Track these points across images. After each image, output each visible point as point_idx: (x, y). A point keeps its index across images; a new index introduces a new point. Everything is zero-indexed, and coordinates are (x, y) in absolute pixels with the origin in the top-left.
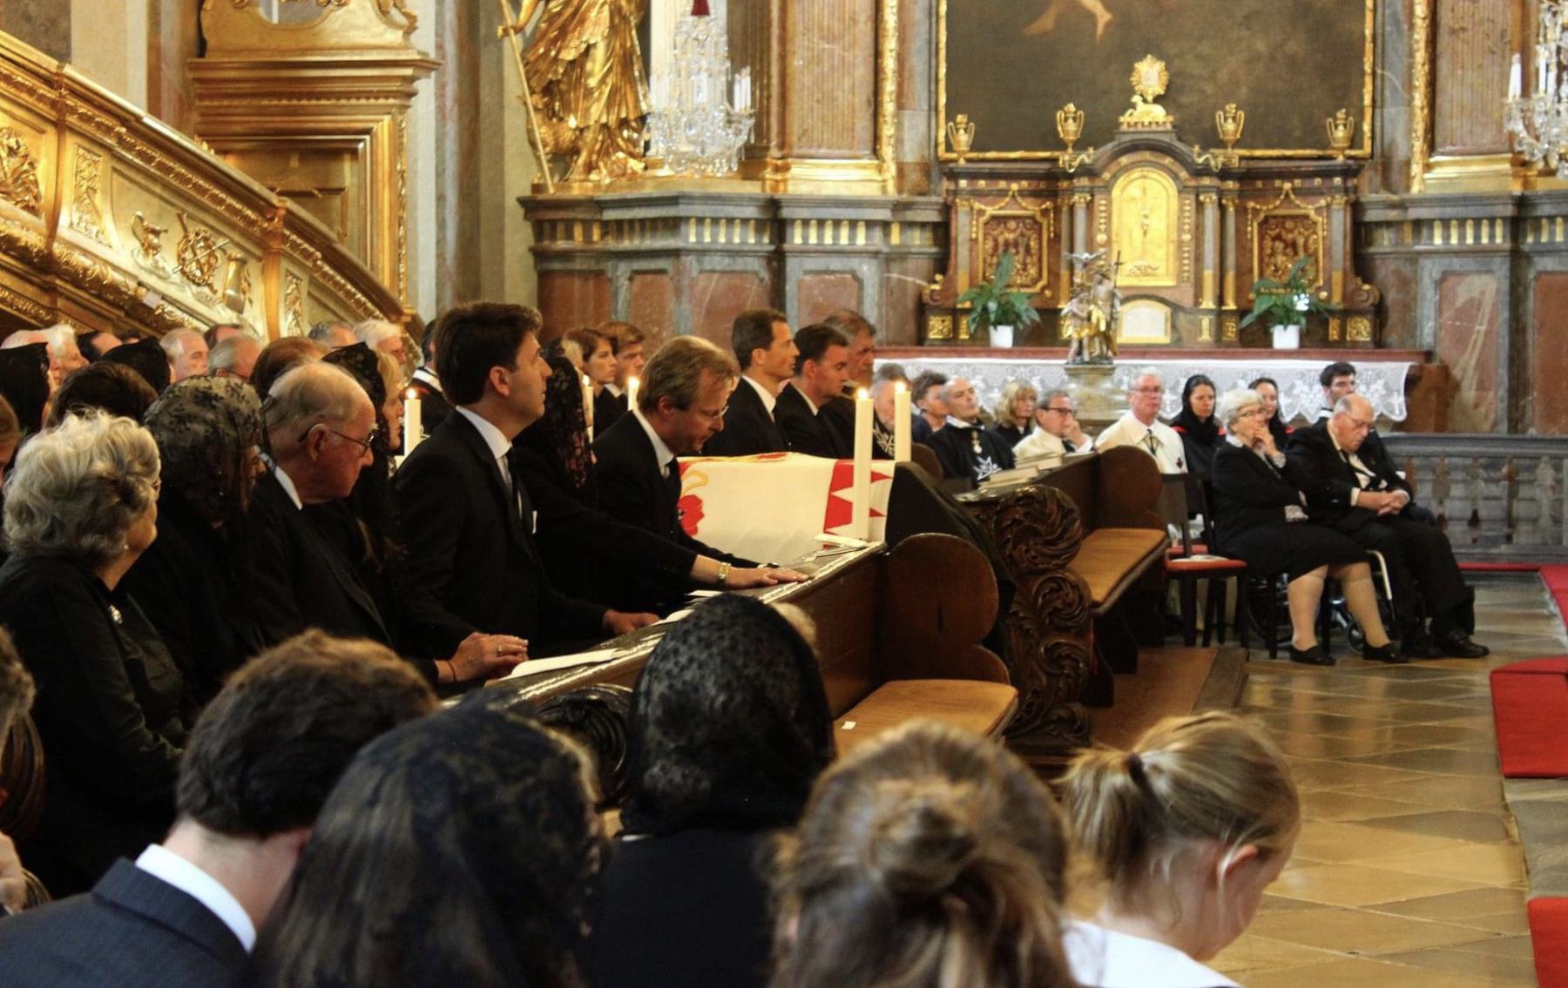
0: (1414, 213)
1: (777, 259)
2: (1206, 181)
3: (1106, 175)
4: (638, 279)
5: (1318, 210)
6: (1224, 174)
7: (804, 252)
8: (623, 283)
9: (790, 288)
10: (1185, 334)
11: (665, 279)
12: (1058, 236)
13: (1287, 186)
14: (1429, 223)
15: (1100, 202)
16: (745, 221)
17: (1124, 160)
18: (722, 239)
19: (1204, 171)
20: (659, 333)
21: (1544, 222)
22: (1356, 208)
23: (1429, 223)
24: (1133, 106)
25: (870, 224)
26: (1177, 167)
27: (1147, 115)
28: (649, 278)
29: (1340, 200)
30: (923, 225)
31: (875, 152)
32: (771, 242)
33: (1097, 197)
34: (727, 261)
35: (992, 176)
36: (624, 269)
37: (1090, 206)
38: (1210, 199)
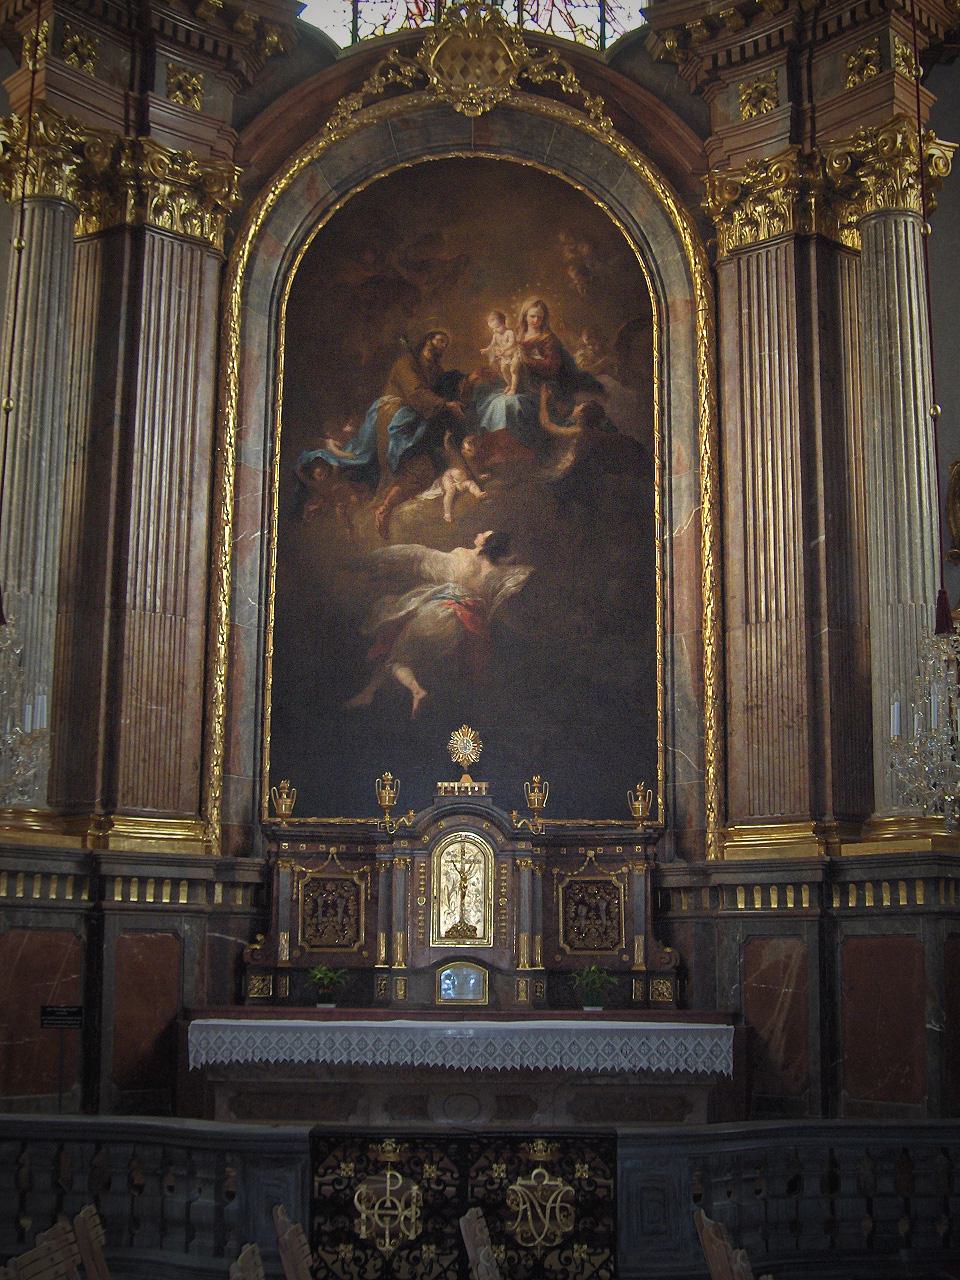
0: (716, 879)
2: (522, 845)
5: (620, 877)
6: (536, 841)
7: (124, 909)
12: (375, 898)
13: (591, 853)
14: (732, 889)
16: (62, 877)
17: (443, 823)
19: (515, 836)
21: (852, 887)
22: (655, 875)
23: (732, 889)
25: (192, 883)
26: (494, 830)
29: (640, 869)
30: (246, 885)
31: (201, 813)
32: (91, 899)
33: (417, 859)
35: (313, 839)
37: (411, 868)
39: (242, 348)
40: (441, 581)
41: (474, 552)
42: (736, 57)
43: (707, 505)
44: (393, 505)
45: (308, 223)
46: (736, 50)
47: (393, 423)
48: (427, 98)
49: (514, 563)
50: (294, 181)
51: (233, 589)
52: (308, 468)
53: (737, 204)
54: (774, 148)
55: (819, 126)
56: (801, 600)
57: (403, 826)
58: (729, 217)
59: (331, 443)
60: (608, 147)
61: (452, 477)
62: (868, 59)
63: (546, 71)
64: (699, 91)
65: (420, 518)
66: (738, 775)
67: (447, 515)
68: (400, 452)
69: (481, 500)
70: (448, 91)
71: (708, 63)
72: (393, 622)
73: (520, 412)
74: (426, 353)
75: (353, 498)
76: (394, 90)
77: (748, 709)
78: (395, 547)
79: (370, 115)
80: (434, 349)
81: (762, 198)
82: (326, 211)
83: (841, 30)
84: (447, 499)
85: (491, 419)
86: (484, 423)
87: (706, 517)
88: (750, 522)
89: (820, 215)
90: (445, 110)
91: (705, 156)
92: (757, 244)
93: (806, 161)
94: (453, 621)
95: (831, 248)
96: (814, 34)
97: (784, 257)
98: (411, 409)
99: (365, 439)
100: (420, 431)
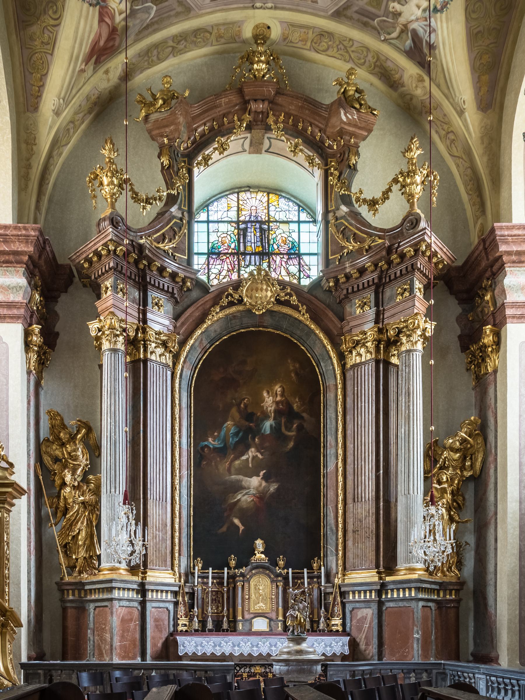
1: (143, 604)
2: (280, 578)
3: (248, 576)
4: (97, 609)
8: (92, 610)
9: (148, 613)
10: (273, 629)
11: (107, 609)
14: (348, 592)
15: (246, 585)
18: (126, 595)
20: (105, 627)
24: (255, 555)
26: (270, 574)
27: (260, 556)
28: (101, 608)
31: (172, 569)
33: (245, 583)
34: (128, 603)
36: (92, 606)
38: (280, 584)
40: (249, 488)
41: (260, 478)
42: (355, 289)
43: (340, 460)
44: (233, 461)
45: (200, 356)
46: (356, 286)
48: (241, 308)
49: (273, 482)
50: (196, 340)
51: (180, 492)
52: (203, 448)
53: (354, 347)
54: (369, 327)
55: (385, 317)
56: (374, 493)
57: (241, 573)
58: (351, 352)
59: (210, 439)
60: (307, 326)
61: (252, 451)
62: (405, 290)
63: (286, 295)
64: (340, 302)
65: (241, 466)
66: (350, 555)
67: (250, 465)
68: (234, 442)
69: (262, 459)
70: (250, 304)
71: (345, 292)
72: (234, 502)
73: (275, 427)
75: (218, 459)
76: (231, 304)
77: (354, 532)
78: (233, 477)
79: (221, 315)
80: (245, 404)
81: (364, 345)
83: (396, 278)
84: (250, 459)
85: (265, 430)
86: (263, 431)
87: (340, 464)
88: (356, 466)
89: (385, 351)
90: (249, 312)
91: (342, 328)
92: (361, 364)
93: (380, 331)
94: (253, 502)
95: (387, 364)
96: (385, 280)
97: (370, 368)
98: (238, 427)
99: (222, 438)
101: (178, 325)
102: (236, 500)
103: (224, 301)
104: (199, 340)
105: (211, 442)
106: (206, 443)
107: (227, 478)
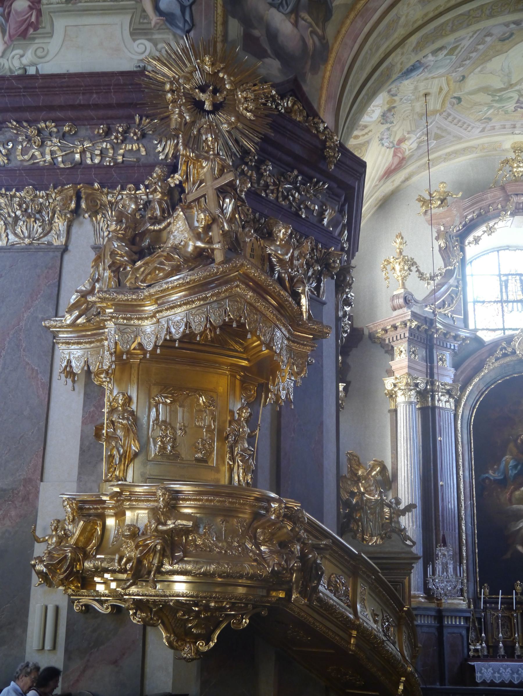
39: (462, 442)
47: (510, 465)
48: (514, 358)
50: (474, 386)
52: (484, 480)
59: (490, 472)
68: (513, 475)
74: (519, 441)
75: (499, 490)
76: (505, 355)
78: (514, 506)
79: (496, 364)
82: (482, 394)
100: (519, 467)
101: (458, 373)
102: (518, 528)
103: (499, 353)
104: (477, 385)
105: (492, 475)
106: (487, 475)
107: (509, 507)
